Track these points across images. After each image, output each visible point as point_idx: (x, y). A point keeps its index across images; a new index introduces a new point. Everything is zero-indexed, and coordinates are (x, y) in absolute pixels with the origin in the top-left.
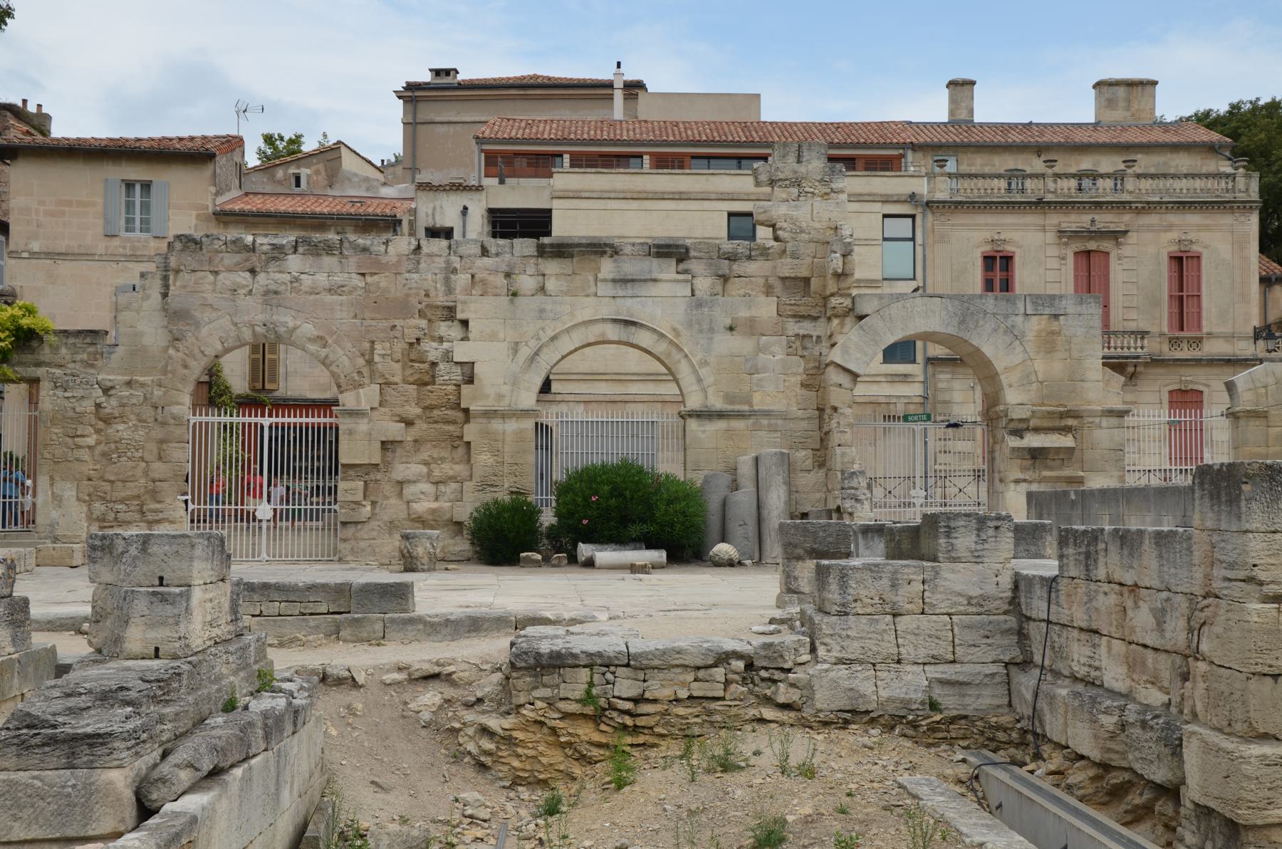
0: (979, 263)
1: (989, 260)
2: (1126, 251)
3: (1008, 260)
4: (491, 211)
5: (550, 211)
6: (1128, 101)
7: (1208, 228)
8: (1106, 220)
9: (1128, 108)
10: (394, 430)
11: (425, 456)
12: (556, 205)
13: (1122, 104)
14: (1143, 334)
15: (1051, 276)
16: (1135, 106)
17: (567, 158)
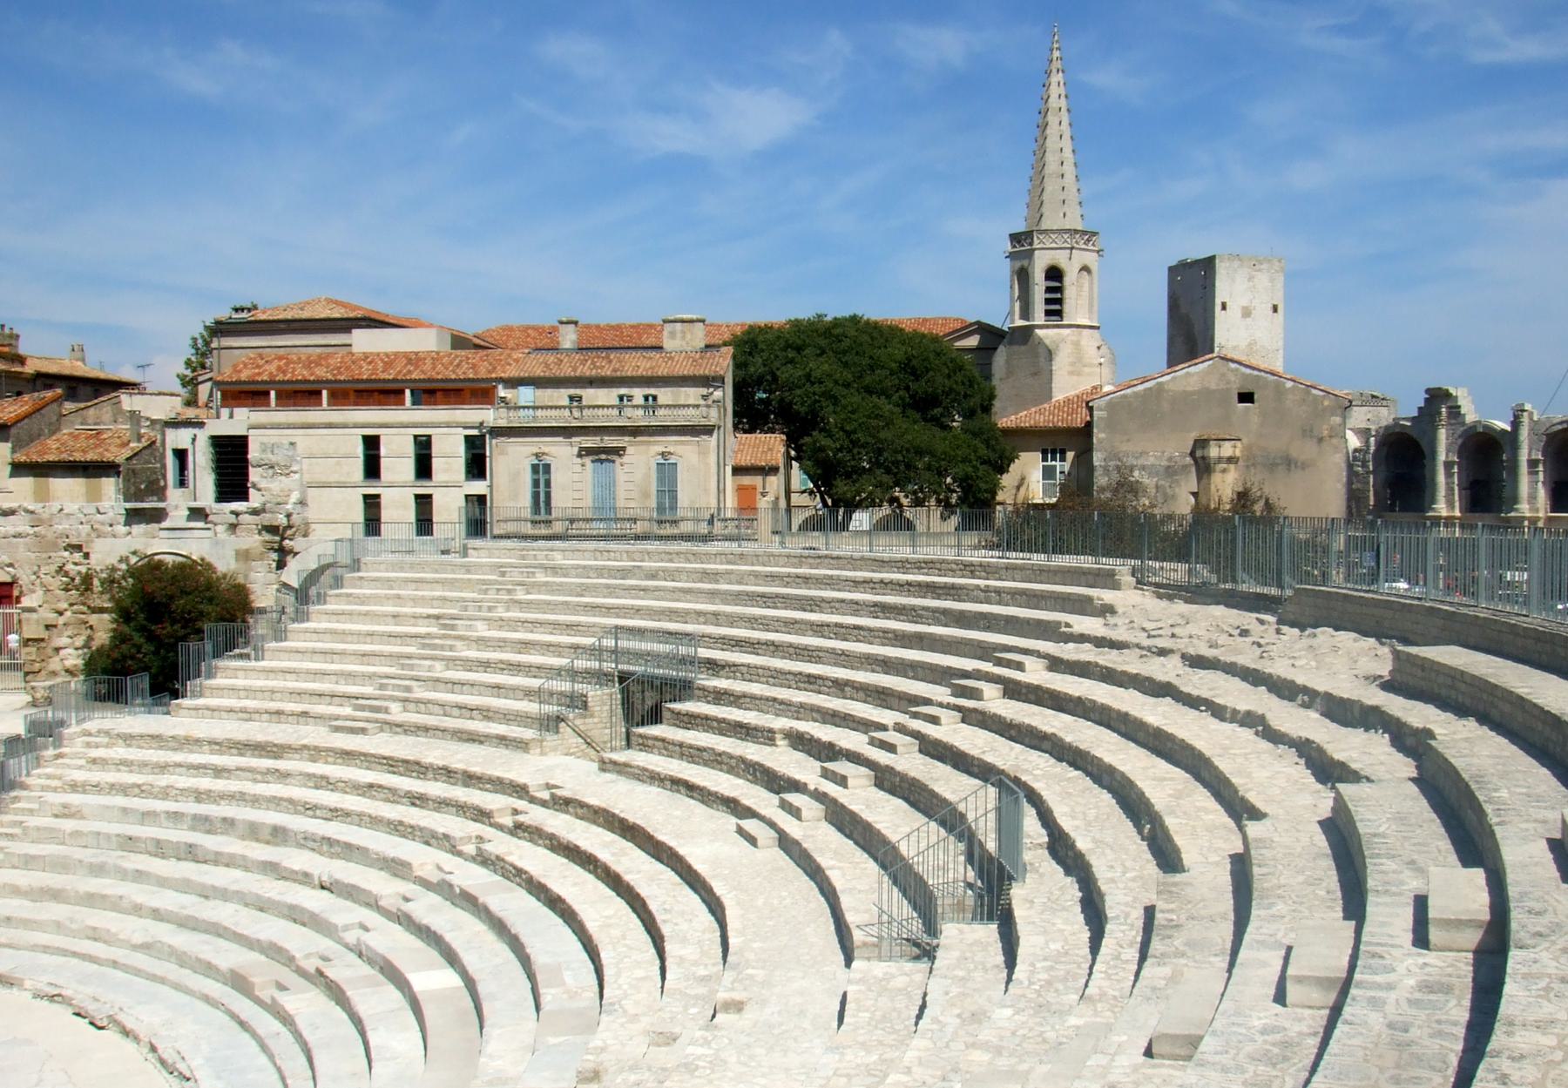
0: (529, 469)
1: (535, 468)
2: (625, 459)
3: (547, 468)
4: (213, 438)
5: (245, 438)
6: (683, 332)
7: (682, 443)
8: (610, 441)
9: (683, 338)
10: (51, 617)
11: (69, 633)
12: (252, 432)
13: (679, 335)
14: (635, 520)
15: (576, 477)
16: (689, 336)
17: (273, 394)
